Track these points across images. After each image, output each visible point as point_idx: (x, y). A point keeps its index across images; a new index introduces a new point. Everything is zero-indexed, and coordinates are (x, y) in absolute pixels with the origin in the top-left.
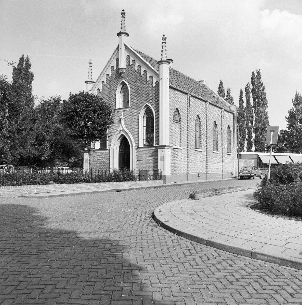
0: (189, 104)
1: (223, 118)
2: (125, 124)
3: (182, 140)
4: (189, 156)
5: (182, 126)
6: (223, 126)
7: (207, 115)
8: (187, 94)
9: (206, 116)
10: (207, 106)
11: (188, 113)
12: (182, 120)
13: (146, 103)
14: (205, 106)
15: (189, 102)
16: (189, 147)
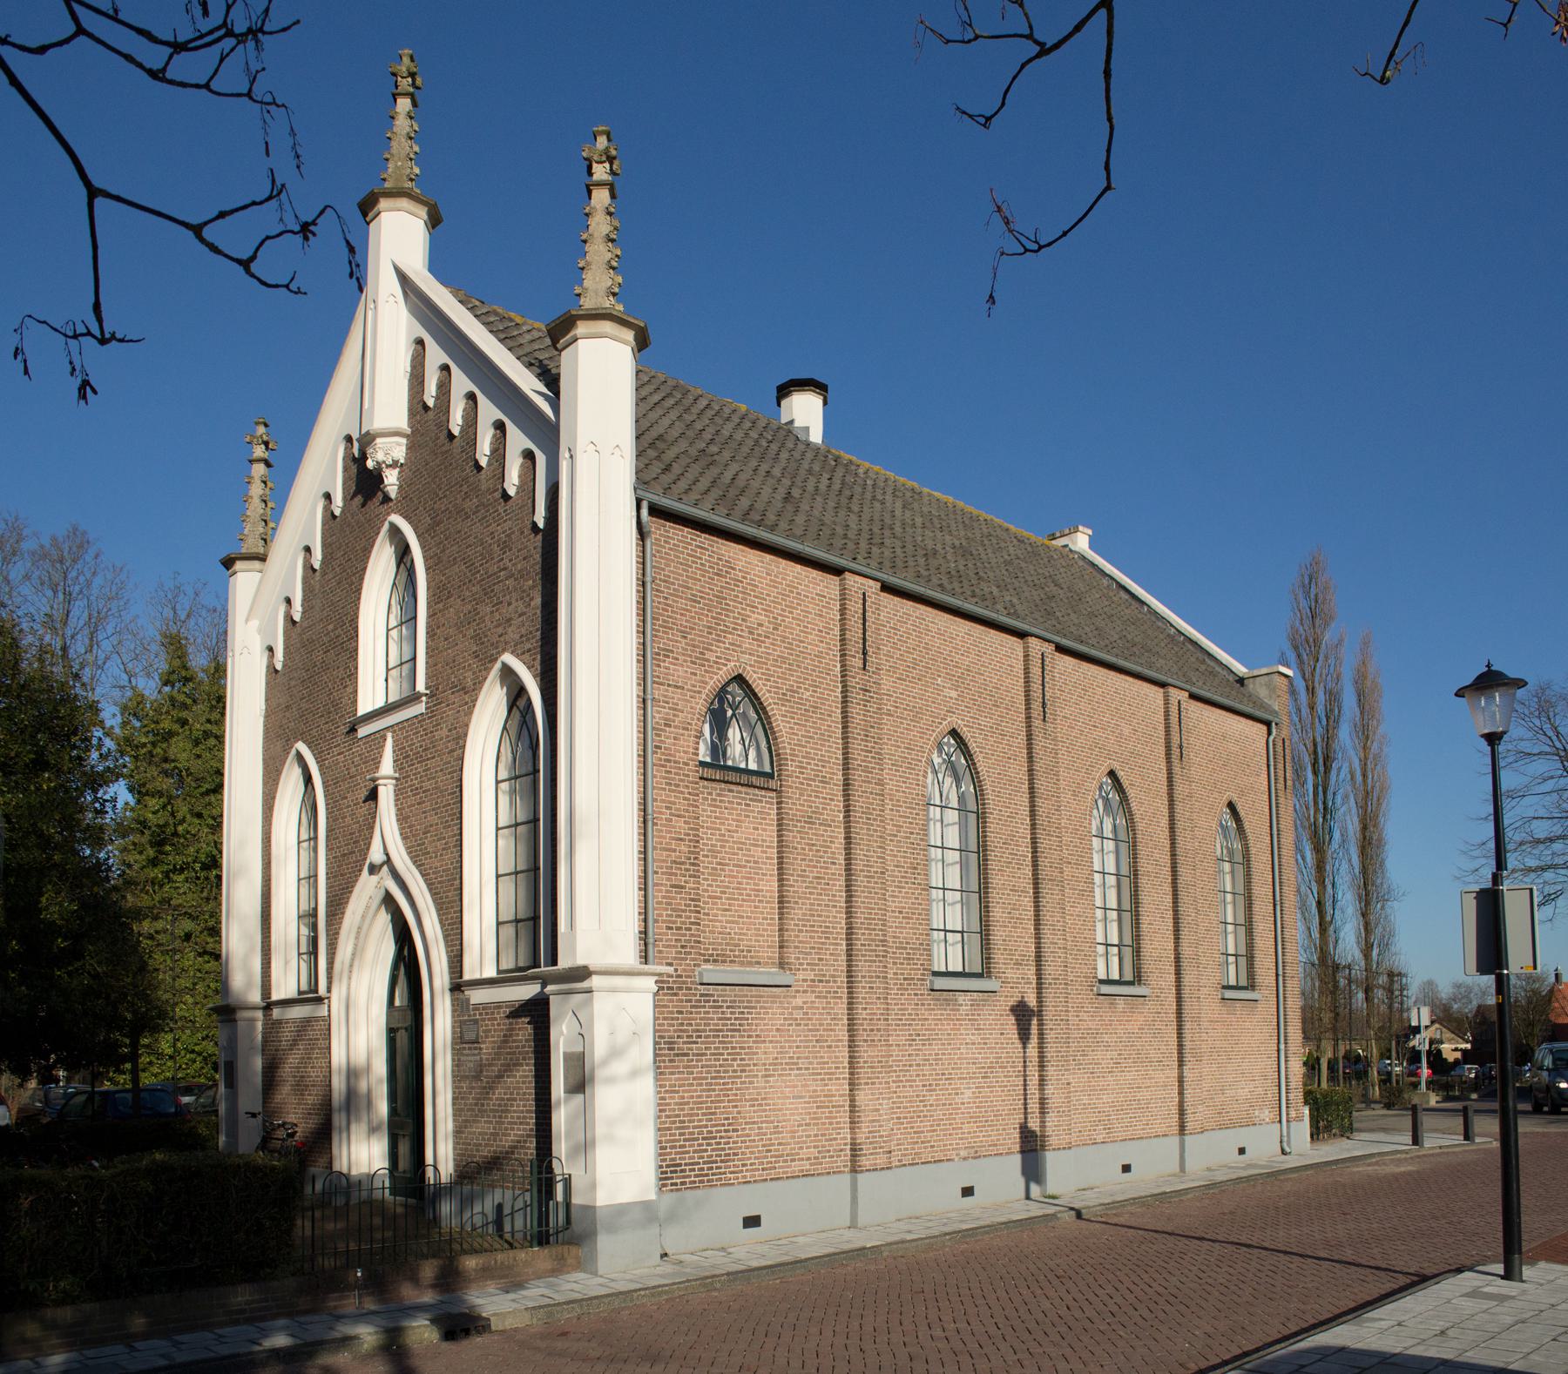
0: (854, 648)
1: (1175, 752)
2: (402, 818)
3: (796, 913)
4: (862, 1036)
5: (796, 804)
6: (1179, 808)
7: (1035, 731)
8: (838, 571)
9: (1029, 737)
10: (1036, 671)
11: (855, 710)
12: (791, 767)
13: (500, 654)
14: (1020, 666)
15: (855, 634)
16: (862, 966)
